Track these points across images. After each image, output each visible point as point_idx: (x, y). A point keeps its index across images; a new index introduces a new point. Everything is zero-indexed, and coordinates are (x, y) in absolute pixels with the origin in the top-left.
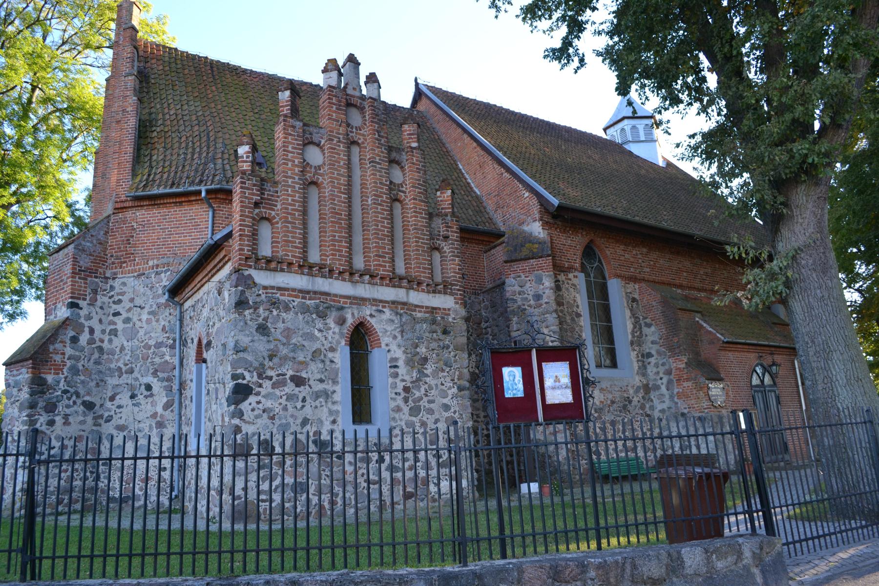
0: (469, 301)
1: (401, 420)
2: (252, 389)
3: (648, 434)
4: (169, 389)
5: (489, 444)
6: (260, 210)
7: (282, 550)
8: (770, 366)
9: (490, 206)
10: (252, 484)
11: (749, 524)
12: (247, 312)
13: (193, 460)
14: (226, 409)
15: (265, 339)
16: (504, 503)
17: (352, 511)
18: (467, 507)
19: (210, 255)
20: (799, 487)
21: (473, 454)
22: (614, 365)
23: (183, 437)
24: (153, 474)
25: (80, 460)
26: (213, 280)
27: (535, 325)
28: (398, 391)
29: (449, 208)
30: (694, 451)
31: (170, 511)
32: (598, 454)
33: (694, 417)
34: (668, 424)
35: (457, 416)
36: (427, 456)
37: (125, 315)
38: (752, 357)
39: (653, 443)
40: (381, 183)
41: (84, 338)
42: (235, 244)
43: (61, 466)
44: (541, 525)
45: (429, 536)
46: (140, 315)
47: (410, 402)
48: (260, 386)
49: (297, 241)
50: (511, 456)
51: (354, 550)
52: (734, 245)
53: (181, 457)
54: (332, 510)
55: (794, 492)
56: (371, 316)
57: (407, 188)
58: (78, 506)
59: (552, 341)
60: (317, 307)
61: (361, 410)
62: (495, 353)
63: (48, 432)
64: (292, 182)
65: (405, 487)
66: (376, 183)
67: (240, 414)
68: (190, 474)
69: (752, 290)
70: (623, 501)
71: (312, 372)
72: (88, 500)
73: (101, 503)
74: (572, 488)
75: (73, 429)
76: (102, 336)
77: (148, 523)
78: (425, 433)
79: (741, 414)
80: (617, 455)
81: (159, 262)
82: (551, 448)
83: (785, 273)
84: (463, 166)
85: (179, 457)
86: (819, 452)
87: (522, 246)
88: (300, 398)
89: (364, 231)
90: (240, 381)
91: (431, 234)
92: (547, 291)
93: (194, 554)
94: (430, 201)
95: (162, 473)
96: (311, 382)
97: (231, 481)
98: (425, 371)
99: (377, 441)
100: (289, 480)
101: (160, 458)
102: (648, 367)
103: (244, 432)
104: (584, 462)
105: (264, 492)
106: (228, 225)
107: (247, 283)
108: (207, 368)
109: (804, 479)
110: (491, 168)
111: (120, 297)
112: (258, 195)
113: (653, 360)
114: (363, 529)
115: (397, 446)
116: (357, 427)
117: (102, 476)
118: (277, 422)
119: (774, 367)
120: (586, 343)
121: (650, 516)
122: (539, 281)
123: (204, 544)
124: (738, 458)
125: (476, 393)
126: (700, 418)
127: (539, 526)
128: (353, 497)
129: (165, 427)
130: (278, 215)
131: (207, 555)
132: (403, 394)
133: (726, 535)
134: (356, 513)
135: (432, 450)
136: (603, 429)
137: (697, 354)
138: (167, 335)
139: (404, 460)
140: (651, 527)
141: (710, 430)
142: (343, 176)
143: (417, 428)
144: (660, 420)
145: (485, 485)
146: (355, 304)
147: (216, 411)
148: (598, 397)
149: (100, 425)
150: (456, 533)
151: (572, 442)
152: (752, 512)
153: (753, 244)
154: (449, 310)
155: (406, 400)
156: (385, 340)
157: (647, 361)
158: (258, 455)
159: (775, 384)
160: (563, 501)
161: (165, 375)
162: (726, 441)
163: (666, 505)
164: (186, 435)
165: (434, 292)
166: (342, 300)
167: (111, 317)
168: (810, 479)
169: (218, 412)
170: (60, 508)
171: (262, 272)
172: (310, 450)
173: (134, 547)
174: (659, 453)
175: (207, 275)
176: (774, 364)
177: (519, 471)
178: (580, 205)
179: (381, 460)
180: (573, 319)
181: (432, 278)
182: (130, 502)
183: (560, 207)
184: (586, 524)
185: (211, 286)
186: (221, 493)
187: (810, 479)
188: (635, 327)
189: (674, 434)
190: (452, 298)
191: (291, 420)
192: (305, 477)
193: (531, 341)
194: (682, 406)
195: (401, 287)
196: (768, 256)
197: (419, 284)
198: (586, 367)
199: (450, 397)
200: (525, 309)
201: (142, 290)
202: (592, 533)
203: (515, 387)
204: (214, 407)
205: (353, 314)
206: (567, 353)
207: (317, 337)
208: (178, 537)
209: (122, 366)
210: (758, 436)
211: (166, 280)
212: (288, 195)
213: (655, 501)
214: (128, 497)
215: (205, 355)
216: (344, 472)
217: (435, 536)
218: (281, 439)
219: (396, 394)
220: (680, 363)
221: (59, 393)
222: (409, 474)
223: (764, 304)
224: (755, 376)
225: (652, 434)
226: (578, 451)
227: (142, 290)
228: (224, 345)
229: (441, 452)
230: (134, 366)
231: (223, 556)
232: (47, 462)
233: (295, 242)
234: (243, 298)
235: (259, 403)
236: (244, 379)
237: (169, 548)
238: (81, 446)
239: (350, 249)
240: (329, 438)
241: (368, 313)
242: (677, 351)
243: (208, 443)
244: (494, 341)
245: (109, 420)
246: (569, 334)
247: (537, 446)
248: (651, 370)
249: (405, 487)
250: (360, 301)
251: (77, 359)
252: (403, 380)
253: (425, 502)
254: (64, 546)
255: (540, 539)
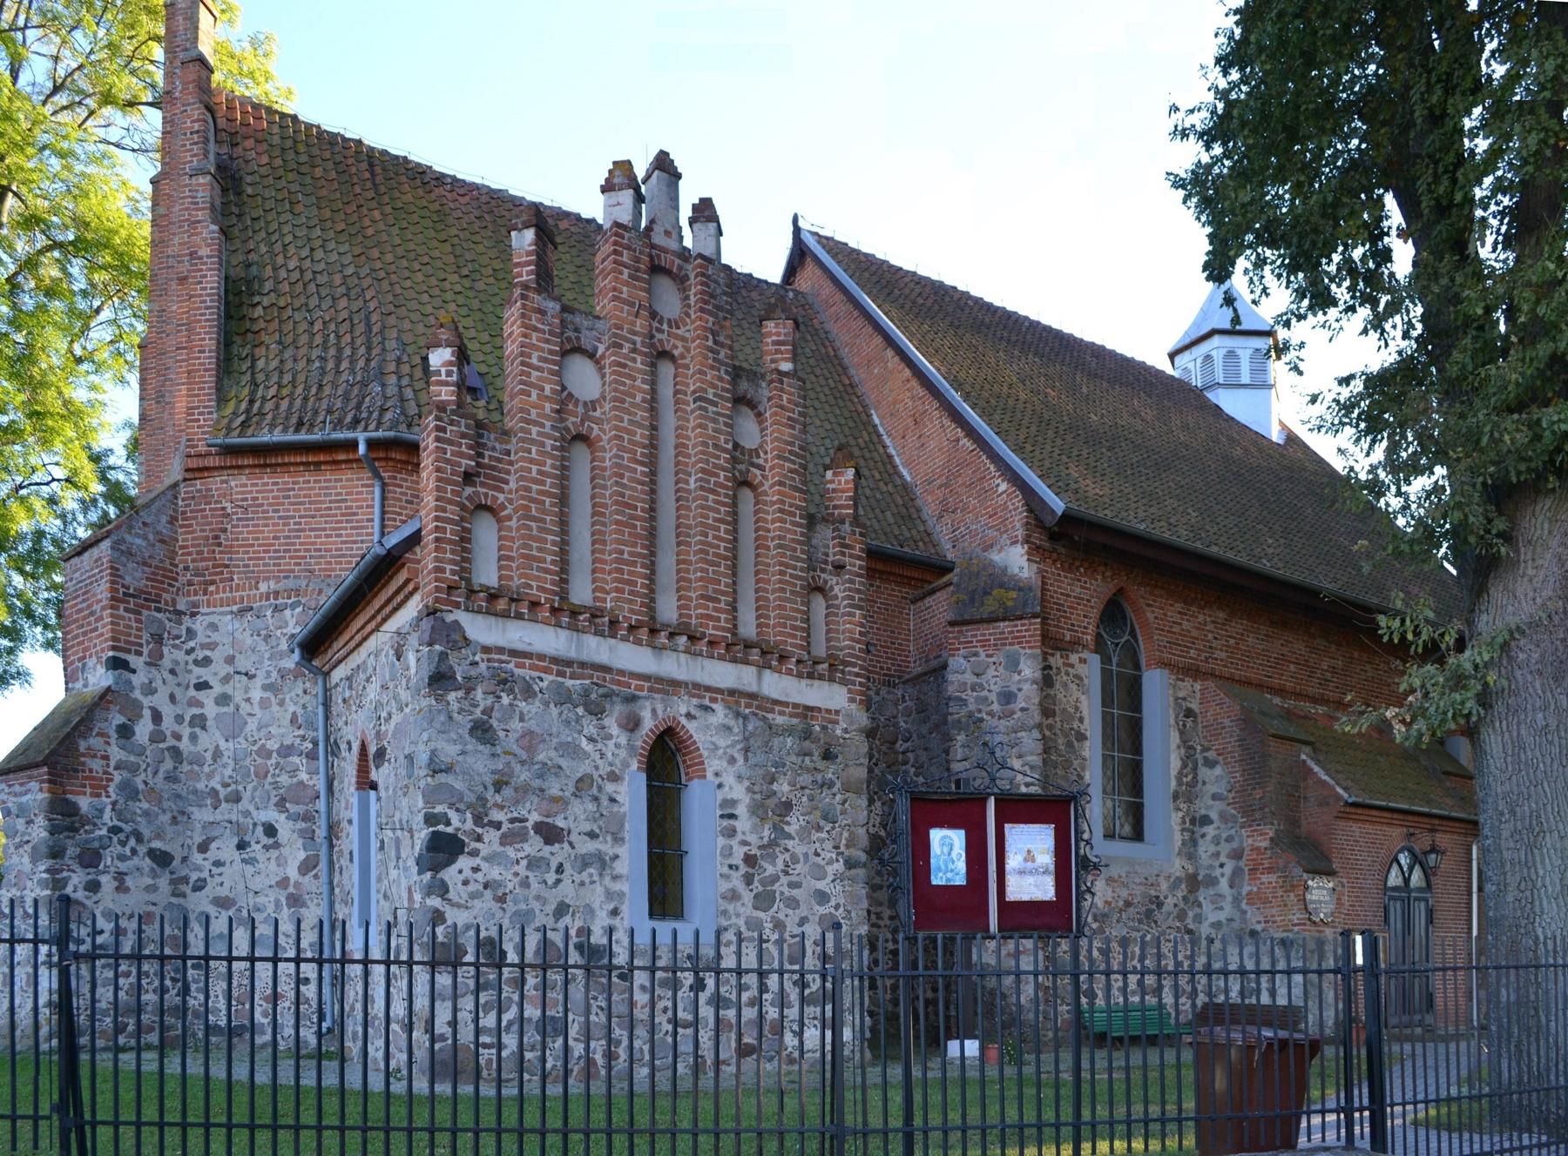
0: (876, 698)
1: (738, 915)
2: (462, 844)
3: (1186, 964)
4: (309, 836)
5: (895, 967)
6: (475, 484)
7: (521, 1132)
8: (1426, 853)
9: (929, 507)
10: (465, 1016)
11: (1343, 1131)
12: (452, 696)
13: (358, 968)
14: (416, 878)
15: (486, 749)
16: (916, 1072)
17: (645, 1071)
18: (849, 1075)
19: (378, 577)
20: (1442, 1073)
21: (866, 984)
22: (1138, 835)
23: (339, 925)
24: (286, 988)
25: (152, 957)
26: (385, 627)
27: (997, 750)
28: (734, 862)
29: (847, 507)
30: (1265, 999)
31: (319, 1056)
32: (1092, 996)
33: (1272, 939)
34: (1224, 950)
35: (840, 913)
36: (782, 983)
37: (218, 689)
38: (1395, 834)
39: (1192, 981)
40: (716, 446)
41: (143, 729)
42: (426, 557)
43: (117, 965)
44: (979, 1113)
45: (780, 1121)
46: (247, 690)
47: (756, 883)
48: (479, 839)
49: (549, 558)
50: (935, 990)
51: (647, 1137)
52: (1395, 614)
53: (336, 961)
54: (609, 1068)
55: (1432, 1080)
56: (689, 716)
57: (768, 459)
58: (153, 1038)
59: (1027, 784)
60: (586, 693)
61: (665, 895)
62: (917, 800)
63: (89, 903)
64: (539, 434)
65: (740, 1036)
66: (705, 444)
67: (442, 890)
68: (354, 991)
69: (1415, 705)
70: (1128, 1079)
71: (576, 817)
72: (170, 1028)
73: (194, 1035)
74: (1039, 1053)
75: (135, 901)
76: (177, 728)
77: (280, 1074)
78: (780, 942)
79: (1359, 939)
80: (1126, 999)
81: (280, 586)
82: (1008, 981)
83: (1484, 677)
84: (882, 418)
85: (332, 961)
86: (1487, 1014)
87: (986, 593)
88: (554, 866)
89: (679, 544)
90: (441, 828)
91: (810, 559)
92: (1026, 687)
93: (365, 1130)
94: (812, 489)
95: (302, 988)
96: (573, 837)
97: (427, 1009)
98: (786, 828)
99: (692, 952)
100: (533, 1012)
101: (298, 960)
102: (1201, 842)
103: (449, 922)
104: (1065, 1008)
105: (488, 1031)
106: (412, 517)
107: (453, 637)
108: (379, 799)
109: (1453, 1058)
110: (939, 428)
111: (208, 653)
112: (470, 458)
113: (1210, 830)
114: (663, 1103)
115: (729, 962)
116: (657, 924)
117: (193, 987)
118: (511, 907)
119: (1433, 856)
120: (1091, 790)
121: (1171, 1108)
122: (1013, 665)
123: (382, 1114)
124: (1341, 1016)
125: (879, 873)
126: (1283, 942)
127: (974, 1114)
128: (646, 1048)
129: (304, 905)
130: (510, 501)
131: (387, 1132)
132: (743, 869)
133: (1300, 1146)
134: (652, 1075)
135: (793, 972)
136: (1106, 952)
137: (1295, 823)
138: (301, 732)
139: (741, 988)
140: (1172, 1127)
141: (1297, 964)
142: (641, 426)
143: (767, 931)
144: (1211, 941)
145: (884, 1038)
146: (658, 691)
147: (397, 881)
148: (1101, 893)
149: (184, 896)
150: (828, 1119)
151: (1046, 972)
152: (1353, 1110)
153: (1431, 615)
154: (837, 712)
155: (748, 880)
156: (713, 765)
157: (1199, 830)
158: (477, 965)
159: (1429, 885)
160: (1020, 1073)
161: (301, 809)
162: (1325, 985)
163: (1203, 1090)
164: (344, 922)
165: (811, 676)
166: (634, 682)
167: (192, 692)
168: (1463, 1060)
169: (400, 883)
170: (122, 1040)
171: (480, 617)
172: (571, 962)
173: (258, 1112)
174: (1202, 999)
175: (373, 617)
176: (1433, 850)
177: (947, 1017)
178: (1106, 515)
179: (699, 986)
180: (1070, 745)
181: (808, 648)
182: (247, 1036)
183: (1067, 518)
184: (1058, 1116)
185: (381, 640)
186: (410, 1028)
187: (1463, 1060)
188: (1184, 766)
189: (1232, 967)
190: (844, 690)
191: (536, 905)
192: (561, 1009)
193: (987, 781)
194: (1254, 919)
195: (747, 663)
196: (1457, 640)
197: (783, 658)
198: (1086, 836)
199: (830, 878)
200: (981, 720)
201: (249, 641)
202: (1066, 1131)
203: (951, 866)
204: (393, 873)
205: (654, 711)
206: (1053, 808)
207: (585, 752)
208: (336, 1100)
209: (218, 787)
210: (1383, 979)
211: (295, 623)
212: (531, 461)
213: (1184, 1082)
214: (243, 1026)
215: (374, 775)
216: (632, 1004)
217: (790, 1121)
218: (517, 939)
219: (731, 867)
220: (1259, 839)
221: (104, 832)
222: (749, 1013)
223: (1433, 734)
224: (1395, 871)
225: (1192, 965)
226: (1055, 987)
227: (249, 641)
228: (410, 758)
229: (809, 977)
230: (240, 788)
231: (416, 1136)
232: (92, 957)
233: (545, 561)
234: (443, 668)
235: (476, 870)
236: (448, 823)
237: (320, 1118)
238: (152, 931)
239: (652, 581)
240: (605, 941)
241: (683, 710)
242: (1258, 815)
243: (384, 938)
244: (918, 779)
245: (199, 886)
246: (1060, 772)
247: (982, 976)
248: (1205, 849)
249: (740, 1036)
250: (668, 686)
251: (134, 769)
252: (744, 843)
253: (776, 1062)
254: (134, 1104)
255: (974, 1136)
